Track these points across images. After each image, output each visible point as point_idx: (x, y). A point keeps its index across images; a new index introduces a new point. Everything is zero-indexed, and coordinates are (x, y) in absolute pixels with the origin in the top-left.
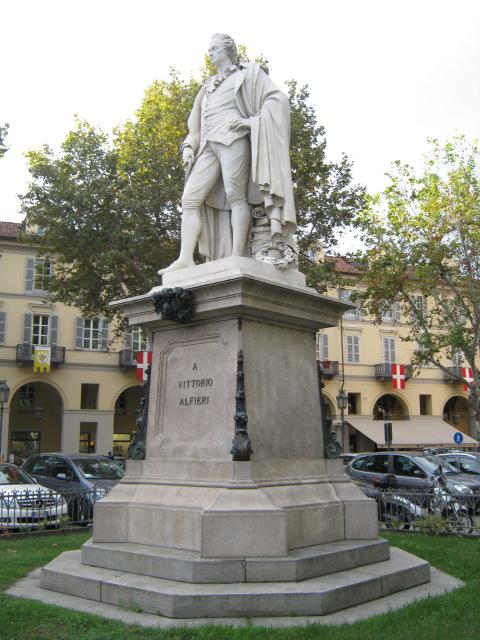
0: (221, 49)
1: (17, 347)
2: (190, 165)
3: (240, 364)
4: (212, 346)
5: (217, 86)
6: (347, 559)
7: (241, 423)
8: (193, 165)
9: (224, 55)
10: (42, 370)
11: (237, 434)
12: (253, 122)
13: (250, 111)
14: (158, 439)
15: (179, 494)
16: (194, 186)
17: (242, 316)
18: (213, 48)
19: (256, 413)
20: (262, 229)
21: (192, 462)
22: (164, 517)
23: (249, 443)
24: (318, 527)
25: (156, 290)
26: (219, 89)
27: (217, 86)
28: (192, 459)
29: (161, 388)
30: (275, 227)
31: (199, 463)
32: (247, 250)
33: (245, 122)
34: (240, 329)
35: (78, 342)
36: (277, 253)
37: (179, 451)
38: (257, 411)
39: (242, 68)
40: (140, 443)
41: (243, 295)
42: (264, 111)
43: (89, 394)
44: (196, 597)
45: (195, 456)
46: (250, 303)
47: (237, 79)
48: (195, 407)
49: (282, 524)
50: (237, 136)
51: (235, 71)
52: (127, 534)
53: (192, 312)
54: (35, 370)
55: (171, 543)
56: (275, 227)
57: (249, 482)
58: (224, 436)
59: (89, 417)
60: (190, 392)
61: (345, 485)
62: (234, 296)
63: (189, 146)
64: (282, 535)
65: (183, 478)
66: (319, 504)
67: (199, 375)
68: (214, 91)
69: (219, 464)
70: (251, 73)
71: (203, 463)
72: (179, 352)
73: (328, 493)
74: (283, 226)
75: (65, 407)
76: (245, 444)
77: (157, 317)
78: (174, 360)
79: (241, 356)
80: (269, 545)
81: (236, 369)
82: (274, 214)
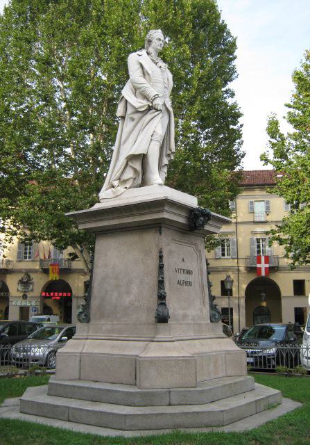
4: (190, 249)
22: (210, 359)
28: (192, 322)
31: (197, 324)
45: (193, 320)
48: (185, 286)
55: (213, 376)
60: (182, 277)
65: (192, 334)
71: (200, 324)
77: (182, 220)
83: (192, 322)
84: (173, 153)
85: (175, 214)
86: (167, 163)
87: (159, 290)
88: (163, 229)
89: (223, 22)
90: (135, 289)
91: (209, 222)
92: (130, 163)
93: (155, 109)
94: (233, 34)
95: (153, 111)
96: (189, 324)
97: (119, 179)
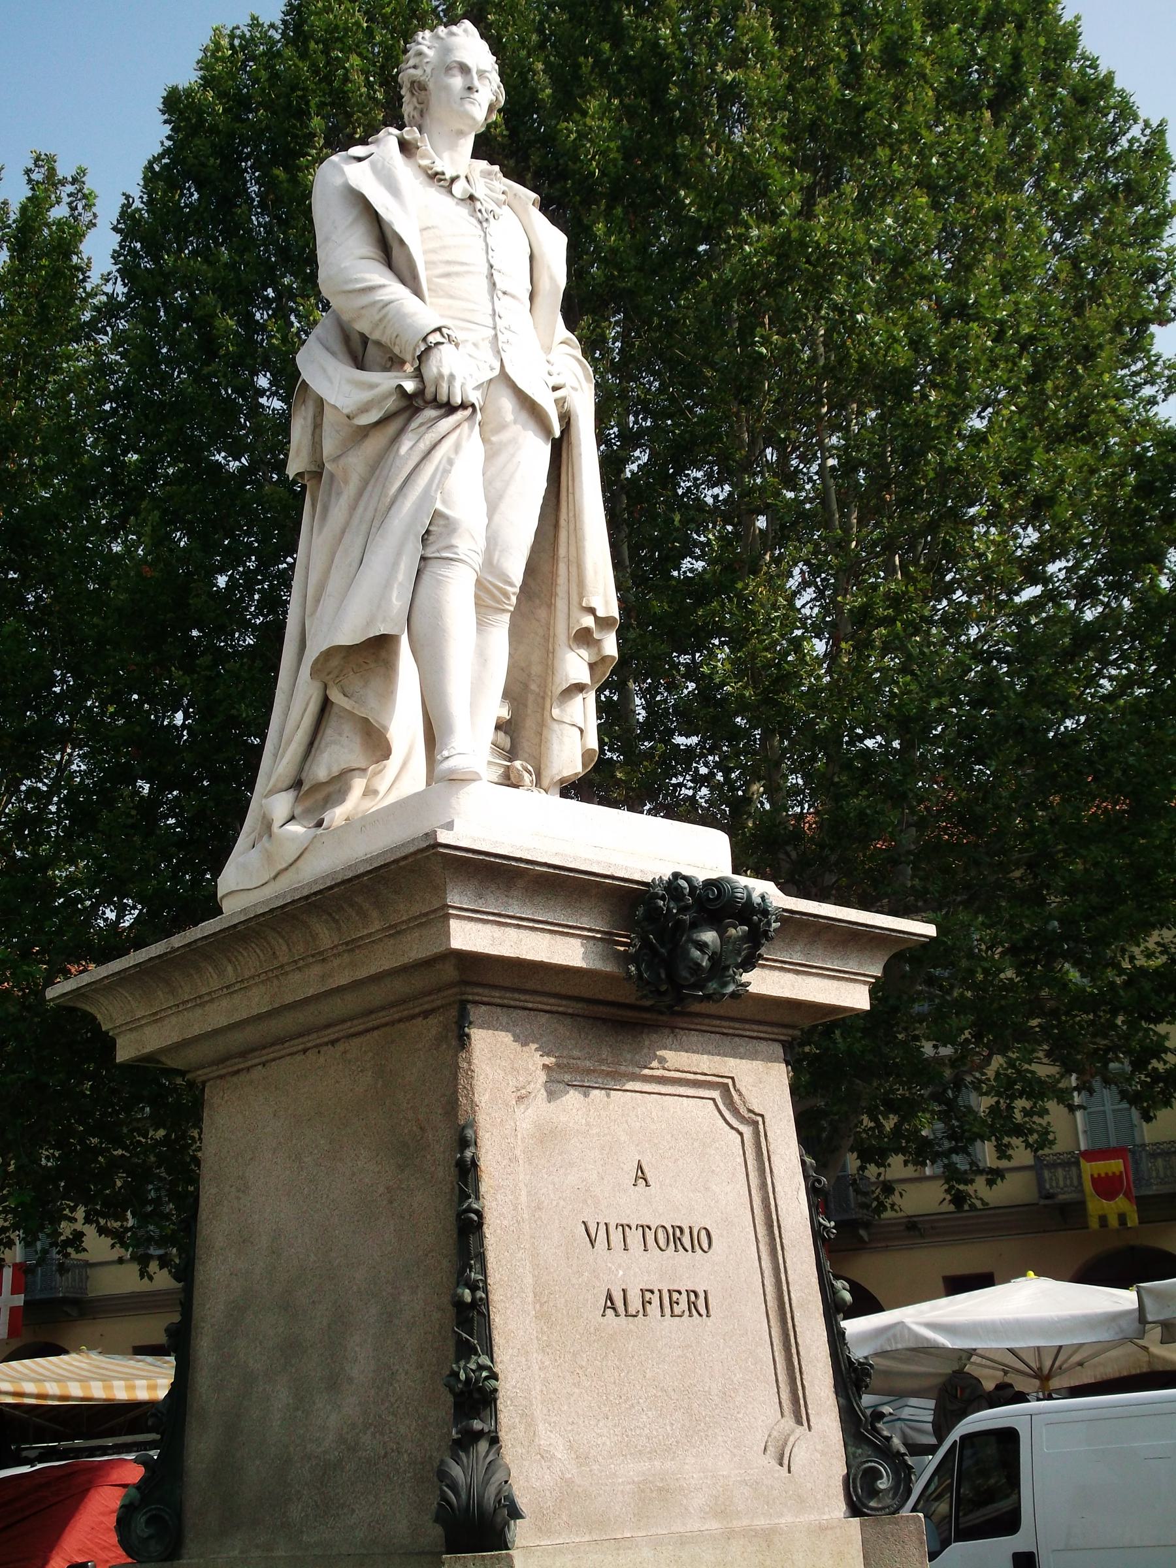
21: (730, 1535)
28: (713, 1525)
31: (752, 1534)
45: (721, 1509)
71: (768, 1536)
77: (569, 952)
83: (713, 1525)
84: (604, 623)
86: (584, 676)
88: (475, 1012)
90: (361, 1363)
91: (762, 951)
92: (336, 696)
93: (435, 403)
94: (1148, 109)
95: (430, 413)
96: (683, 1540)
97: (297, 784)
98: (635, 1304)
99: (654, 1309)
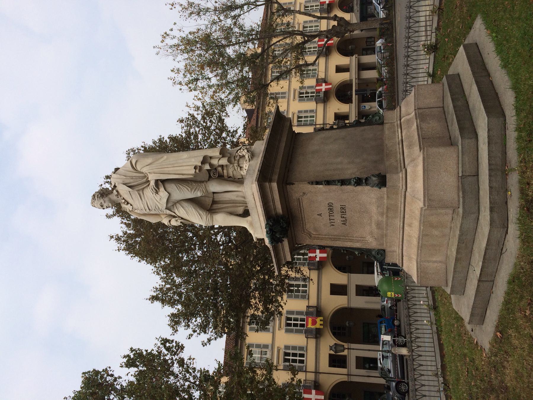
0: (102, 201)
1: (307, 338)
2: (182, 221)
3: (318, 183)
4: (305, 202)
5: (128, 203)
6: (459, 103)
7: (359, 182)
8: (182, 218)
9: (106, 199)
10: (322, 323)
11: (367, 184)
12: (152, 178)
13: (145, 179)
14: (369, 239)
15: (410, 225)
16: (197, 218)
17: (285, 183)
18: (102, 206)
19: (351, 171)
20: (225, 171)
21: (387, 216)
22: (427, 235)
23: (373, 175)
24: (433, 126)
25: (267, 242)
26: (130, 201)
27: (128, 203)
28: (385, 216)
29: (336, 238)
30: (224, 161)
32: (240, 181)
33: (152, 183)
34: (293, 184)
35: (303, 297)
36: (241, 160)
37: (379, 225)
38: (349, 172)
39: (115, 186)
40: (373, 253)
41: (270, 181)
42: (145, 170)
43: (337, 290)
44: (492, 210)
45: (382, 214)
46: (276, 177)
47: (123, 190)
48: (348, 215)
49: (434, 150)
50: (162, 189)
51: (117, 191)
52: (440, 262)
53: (282, 217)
54: (322, 327)
56: (224, 161)
57: (401, 175)
58: (369, 195)
59: (352, 290)
61: (403, 109)
62: (271, 188)
63: (170, 221)
64: (442, 150)
65: (398, 223)
66: (417, 126)
67: (325, 211)
68: (131, 205)
69: (388, 197)
70: (119, 180)
71: (388, 208)
72: (309, 226)
73: (408, 121)
74: (223, 157)
75: (346, 306)
76: (374, 179)
77: (286, 243)
78: (315, 230)
79: (312, 183)
80: (450, 162)
81: (321, 186)
82: (215, 162)
85: (283, 250)
87: (351, 185)
89: (147, 351)
98: (344, 219)
99: (345, 216)
